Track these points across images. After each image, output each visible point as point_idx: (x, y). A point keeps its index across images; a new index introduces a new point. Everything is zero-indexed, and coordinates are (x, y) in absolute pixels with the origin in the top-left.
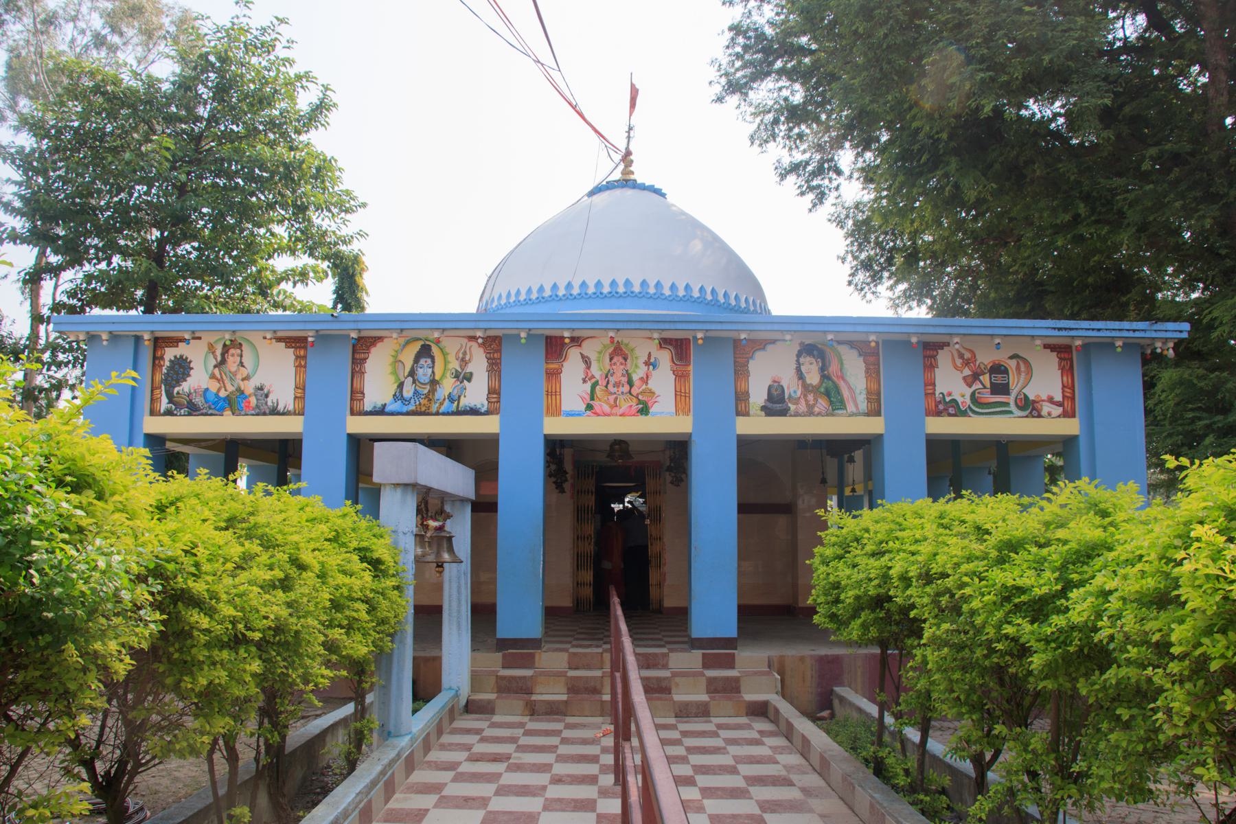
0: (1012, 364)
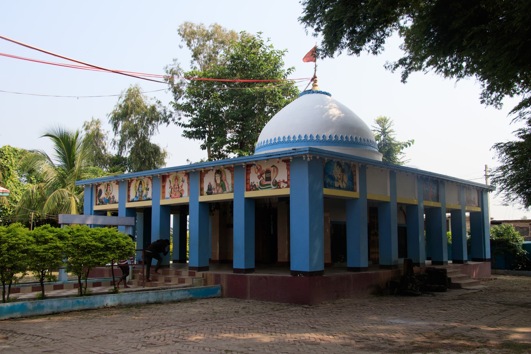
0: (272, 169)
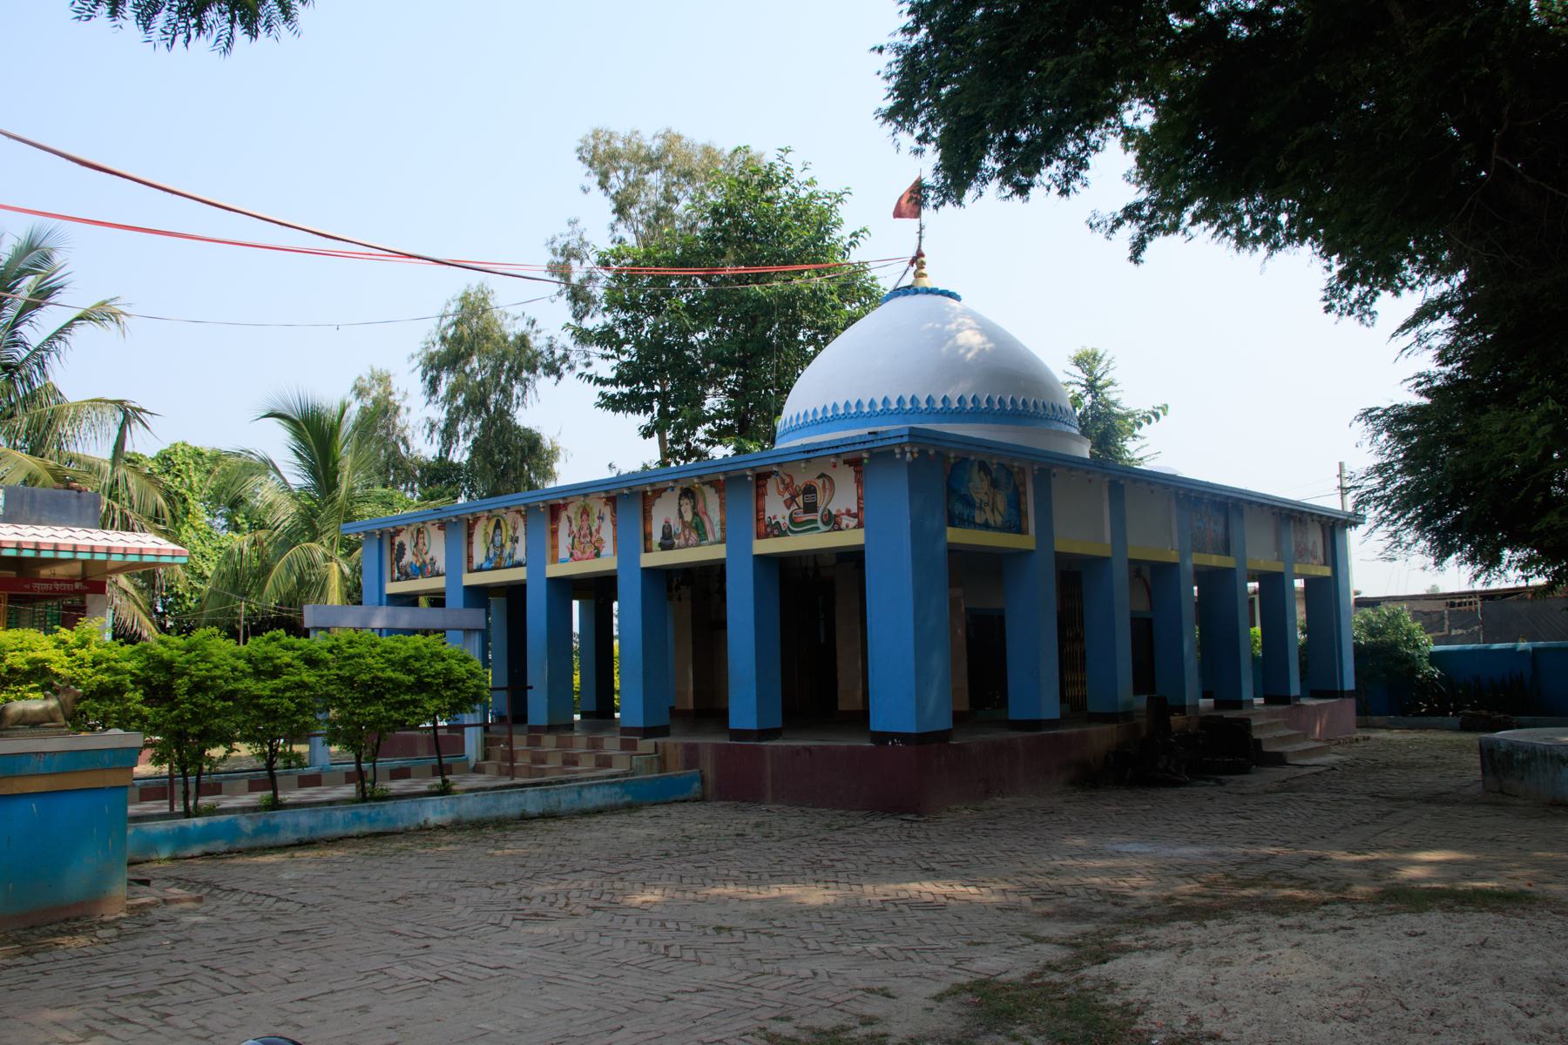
0: (820, 482)
